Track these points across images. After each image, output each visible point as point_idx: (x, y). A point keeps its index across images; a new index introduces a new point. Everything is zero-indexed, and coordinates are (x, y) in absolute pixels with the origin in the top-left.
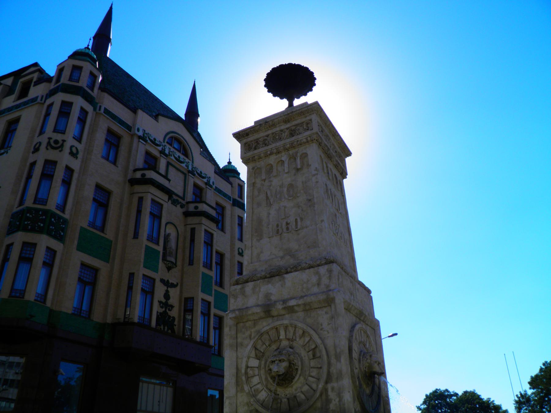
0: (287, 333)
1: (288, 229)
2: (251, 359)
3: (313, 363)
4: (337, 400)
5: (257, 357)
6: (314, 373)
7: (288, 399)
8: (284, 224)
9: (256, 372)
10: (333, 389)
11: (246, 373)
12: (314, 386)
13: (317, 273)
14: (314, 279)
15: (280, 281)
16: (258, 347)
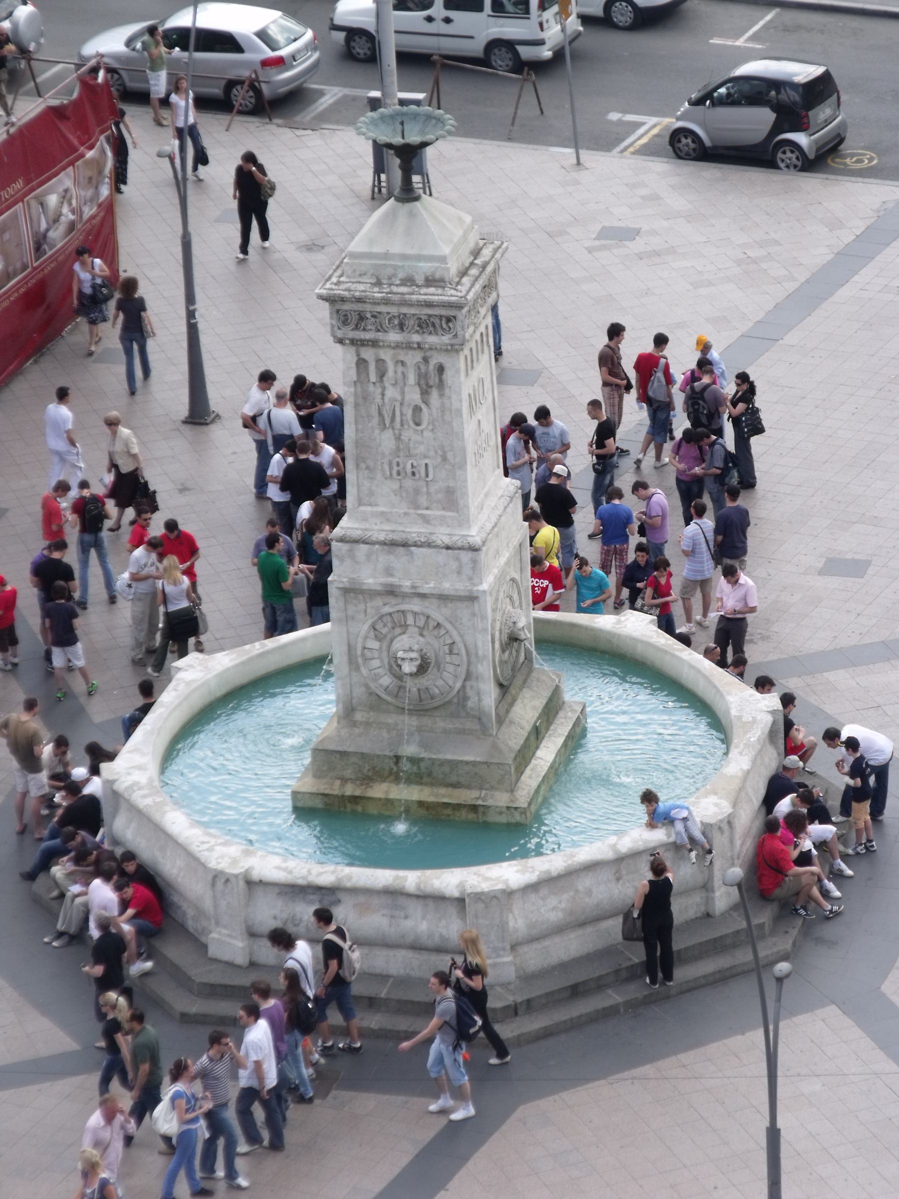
0: (417, 620)
1: (413, 474)
2: (368, 640)
3: (448, 659)
4: (476, 698)
5: (377, 638)
6: (451, 668)
7: (419, 690)
8: (409, 466)
9: (376, 655)
10: (472, 687)
11: (363, 655)
12: (451, 683)
13: (457, 559)
14: (454, 565)
15: (406, 555)
16: (377, 627)
